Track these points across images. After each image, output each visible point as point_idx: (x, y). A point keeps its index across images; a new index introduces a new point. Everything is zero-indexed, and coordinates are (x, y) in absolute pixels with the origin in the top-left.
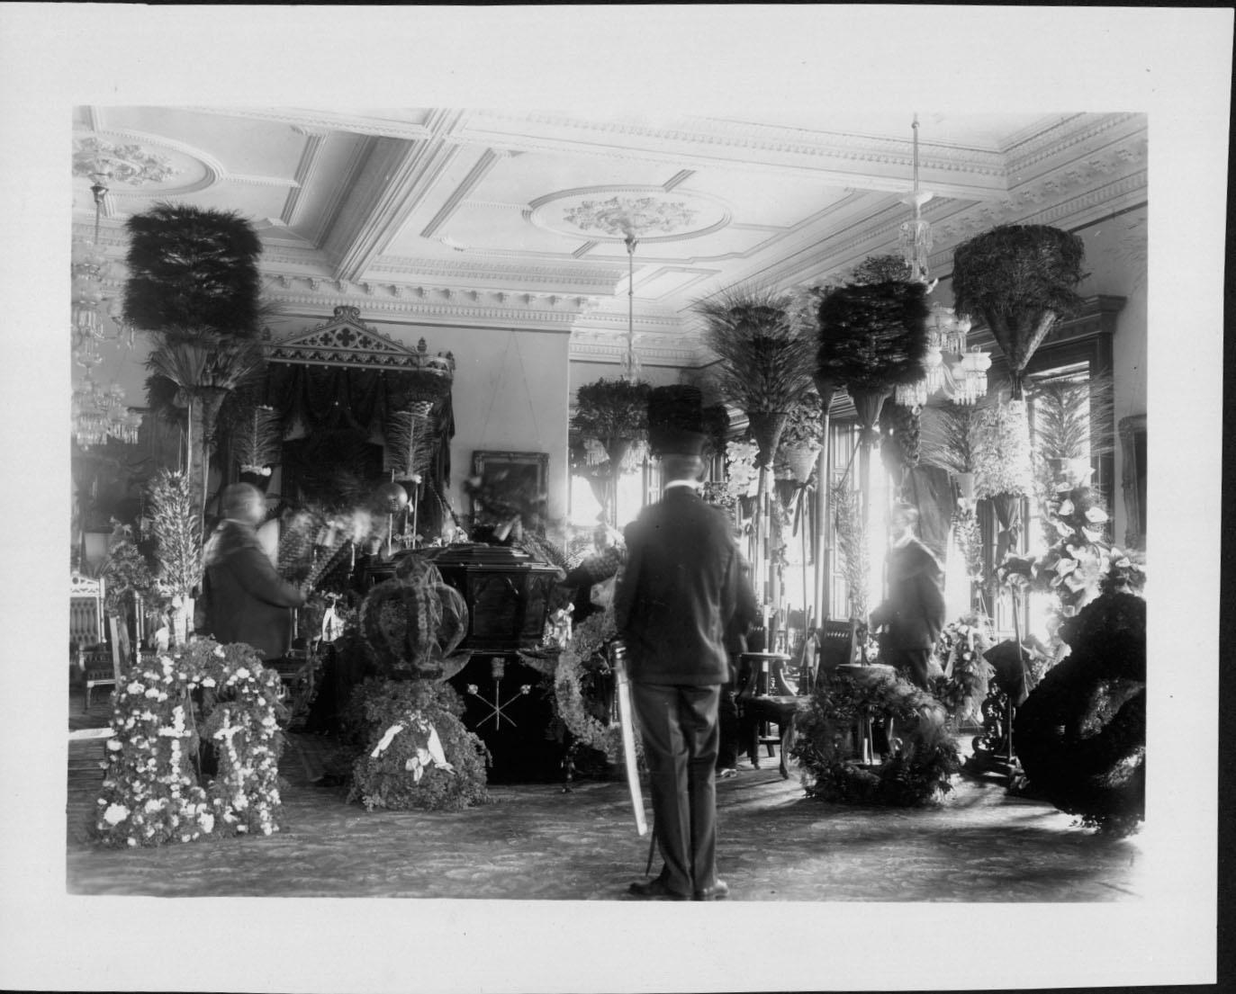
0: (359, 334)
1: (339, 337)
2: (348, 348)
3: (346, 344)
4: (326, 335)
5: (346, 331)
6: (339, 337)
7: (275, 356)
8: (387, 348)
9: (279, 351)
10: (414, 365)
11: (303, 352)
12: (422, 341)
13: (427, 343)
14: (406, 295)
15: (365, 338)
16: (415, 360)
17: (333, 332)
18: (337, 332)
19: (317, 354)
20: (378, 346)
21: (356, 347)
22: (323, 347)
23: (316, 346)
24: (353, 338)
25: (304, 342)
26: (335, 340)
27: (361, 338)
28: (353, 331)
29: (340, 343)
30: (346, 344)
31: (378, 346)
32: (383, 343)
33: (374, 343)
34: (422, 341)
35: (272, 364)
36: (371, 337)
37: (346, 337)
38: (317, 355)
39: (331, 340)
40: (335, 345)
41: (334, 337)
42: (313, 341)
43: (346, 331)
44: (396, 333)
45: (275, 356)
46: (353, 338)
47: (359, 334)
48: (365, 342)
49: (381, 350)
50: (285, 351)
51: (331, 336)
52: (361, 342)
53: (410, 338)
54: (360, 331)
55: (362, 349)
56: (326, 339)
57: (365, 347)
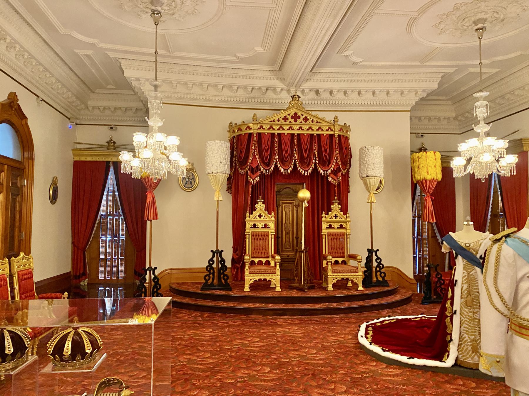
0: (302, 115)
1: (292, 117)
2: (297, 123)
3: (296, 121)
4: (285, 117)
6: (292, 117)
9: (261, 127)
10: (332, 130)
11: (274, 127)
12: (336, 117)
15: (306, 117)
16: (332, 127)
17: (289, 115)
18: (291, 115)
19: (281, 127)
20: (313, 121)
21: (301, 122)
22: (284, 122)
23: (280, 123)
24: (299, 117)
25: (274, 121)
26: (290, 119)
27: (304, 117)
28: (299, 114)
29: (292, 121)
30: (296, 121)
31: (313, 121)
33: (310, 120)
34: (336, 117)
37: (296, 117)
39: (288, 119)
40: (290, 122)
42: (278, 120)
43: (296, 114)
46: (299, 117)
47: (302, 115)
49: (314, 123)
51: (288, 117)
56: (285, 119)
57: (306, 122)
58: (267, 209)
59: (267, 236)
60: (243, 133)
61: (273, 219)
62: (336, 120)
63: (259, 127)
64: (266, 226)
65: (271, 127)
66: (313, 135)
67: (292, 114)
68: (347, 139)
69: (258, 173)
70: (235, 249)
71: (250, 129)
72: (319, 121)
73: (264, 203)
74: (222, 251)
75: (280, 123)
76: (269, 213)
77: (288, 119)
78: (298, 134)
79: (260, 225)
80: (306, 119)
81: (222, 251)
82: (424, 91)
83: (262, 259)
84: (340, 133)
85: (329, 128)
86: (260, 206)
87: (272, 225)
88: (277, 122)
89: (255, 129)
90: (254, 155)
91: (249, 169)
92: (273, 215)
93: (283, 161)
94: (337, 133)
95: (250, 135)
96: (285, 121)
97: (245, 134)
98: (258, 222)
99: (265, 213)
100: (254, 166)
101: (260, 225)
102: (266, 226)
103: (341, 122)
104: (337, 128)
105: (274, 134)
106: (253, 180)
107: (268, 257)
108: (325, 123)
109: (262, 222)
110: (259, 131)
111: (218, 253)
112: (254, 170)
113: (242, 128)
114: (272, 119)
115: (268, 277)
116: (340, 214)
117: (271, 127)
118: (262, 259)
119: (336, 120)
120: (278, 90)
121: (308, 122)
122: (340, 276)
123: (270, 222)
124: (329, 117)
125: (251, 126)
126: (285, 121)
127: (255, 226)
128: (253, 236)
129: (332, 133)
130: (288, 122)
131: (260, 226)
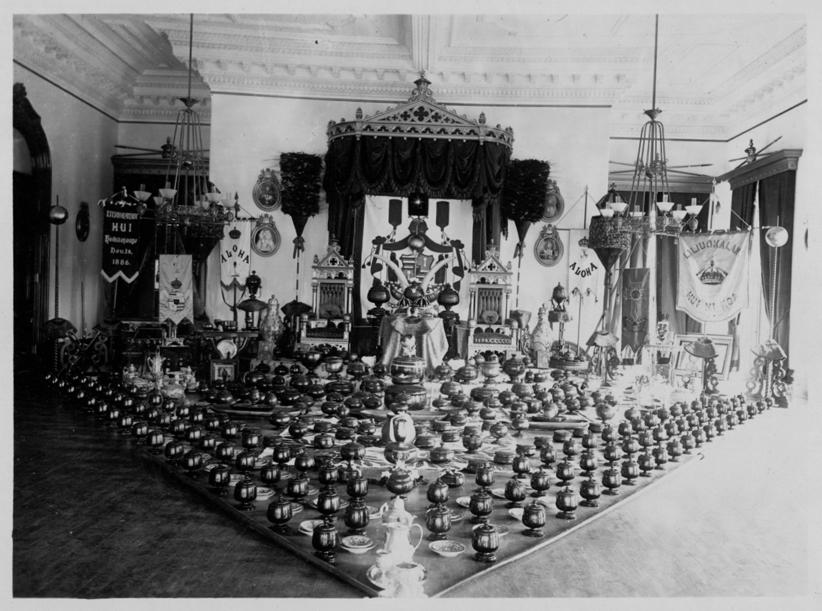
0: (432, 111)
1: (416, 114)
2: (423, 122)
3: (421, 119)
5: (421, 108)
6: (416, 114)
7: (365, 130)
8: (453, 121)
10: (476, 134)
12: (483, 115)
13: (486, 116)
16: (476, 130)
21: (429, 121)
22: (403, 121)
25: (388, 119)
26: (413, 116)
27: (433, 113)
29: (416, 118)
30: (421, 119)
34: (483, 115)
35: (363, 137)
36: (441, 113)
37: (421, 114)
39: (409, 116)
40: (413, 120)
42: (395, 118)
43: (421, 108)
44: (460, 111)
45: (365, 130)
48: (436, 117)
52: (433, 117)
53: (473, 114)
54: (433, 108)
55: (433, 122)
63: (364, 127)
65: (383, 128)
67: (416, 109)
72: (456, 119)
75: (397, 121)
77: (409, 116)
96: (405, 119)
108: (466, 124)
110: (365, 133)
114: (386, 116)
126: (405, 119)
129: (476, 138)
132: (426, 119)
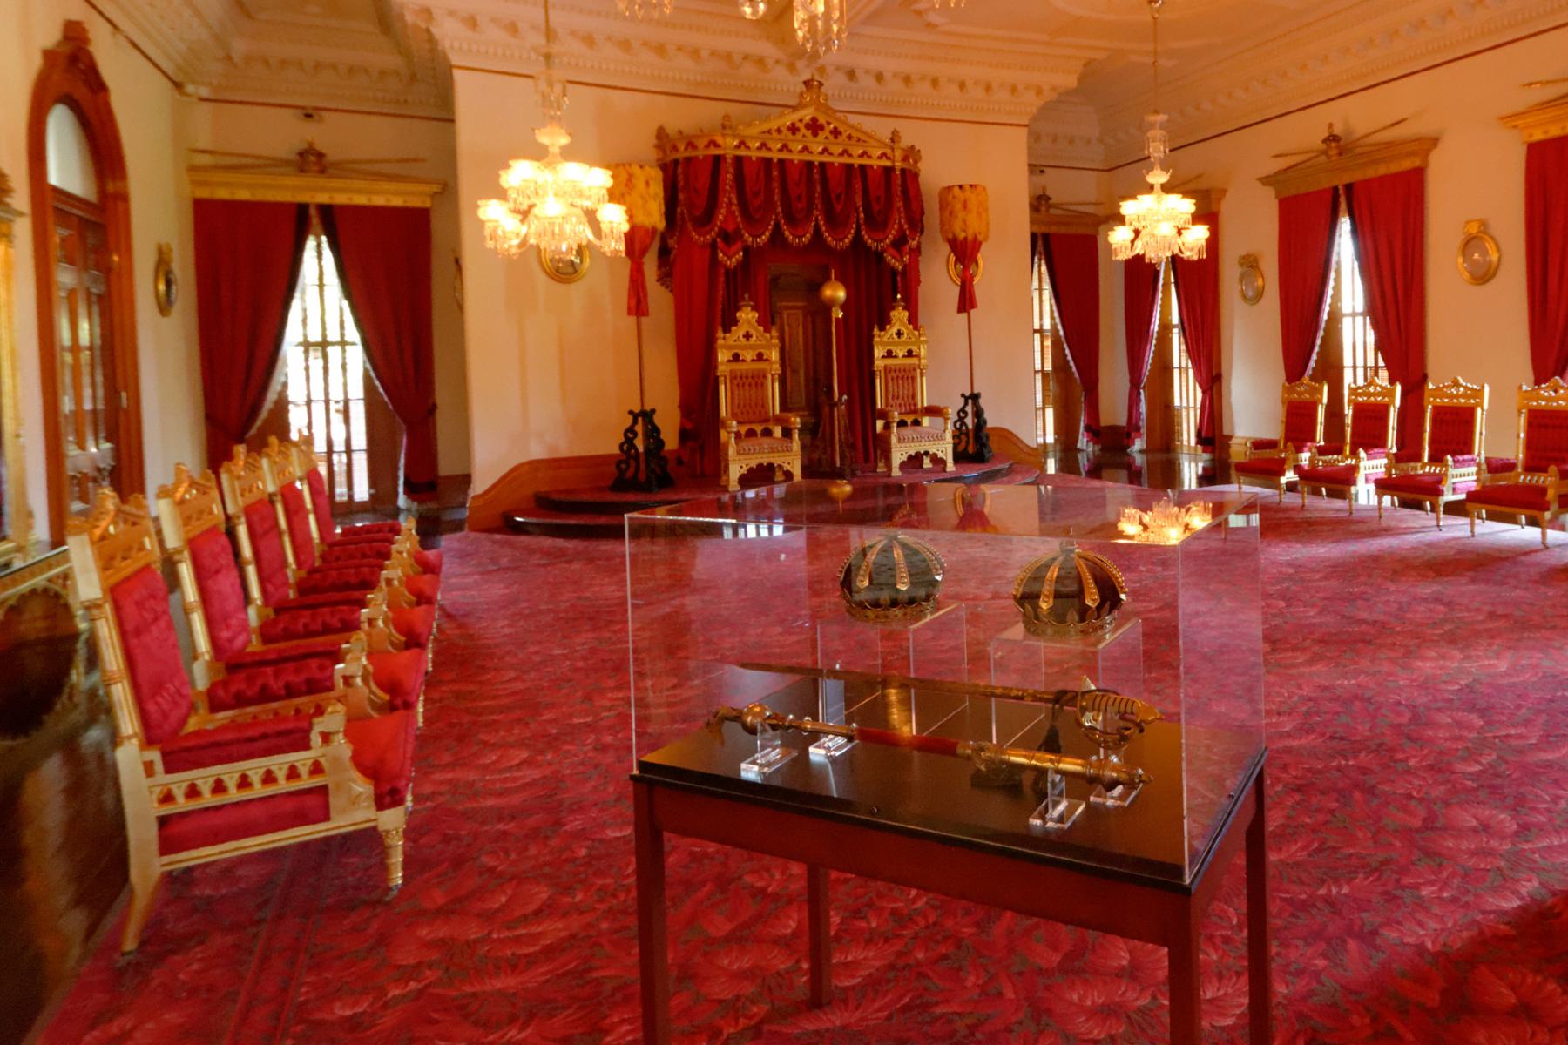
3: (815, 135)
6: (807, 126)
9: (742, 143)
11: (770, 144)
14: (867, 82)
20: (850, 137)
22: (790, 136)
24: (822, 128)
25: (769, 132)
26: (803, 130)
28: (822, 120)
29: (808, 133)
30: (815, 135)
31: (850, 137)
32: (855, 134)
37: (815, 127)
38: (785, 147)
41: (801, 126)
42: (779, 131)
43: (814, 120)
45: (738, 147)
46: (822, 128)
49: (854, 141)
50: (749, 143)
51: (799, 125)
56: (793, 129)
58: (767, 321)
59: (765, 377)
60: (701, 153)
61: (776, 341)
62: (895, 137)
64: (760, 357)
66: (850, 166)
67: (808, 118)
68: (916, 176)
69: (739, 245)
70: (686, 407)
71: (717, 146)
72: (863, 137)
73: (754, 308)
74: (653, 411)
75: (782, 136)
76: (767, 330)
78: (822, 164)
79: (749, 355)
80: (836, 133)
81: (653, 411)
82: (1054, 89)
83: (754, 426)
84: (905, 166)
85: (884, 155)
86: (747, 316)
87: (774, 355)
88: (775, 134)
89: (728, 146)
90: (730, 203)
91: (718, 235)
92: (775, 333)
93: (791, 219)
94: (898, 164)
95: (718, 160)
97: (706, 157)
98: (744, 348)
99: (757, 332)
100: (730, 228)
101: (749, 355)
102: (760, 357)
103: (906, 142)
104: (898, 154)
105: (770, 160)
106: (730, 258)
107: (767, 420)
108: (872, 142)
109: (751, 347)
111: (647, 416)
112: (729, 238)
113: (696, 142)
115: (776, 460)
116: (907, 330)
117: (763, 146)
118: (754, 426)
119: (895, 137)
120: (770, 62)
121: (840, 139)
122: (912, 450)
123: (770, 347)
124: (881, 129)
125: (719, 140)
127: (736, 358)
128: (733, 378)
129: (888, 163)
130: (799, 136)
131: (749, 358)
132: (821, 135)
